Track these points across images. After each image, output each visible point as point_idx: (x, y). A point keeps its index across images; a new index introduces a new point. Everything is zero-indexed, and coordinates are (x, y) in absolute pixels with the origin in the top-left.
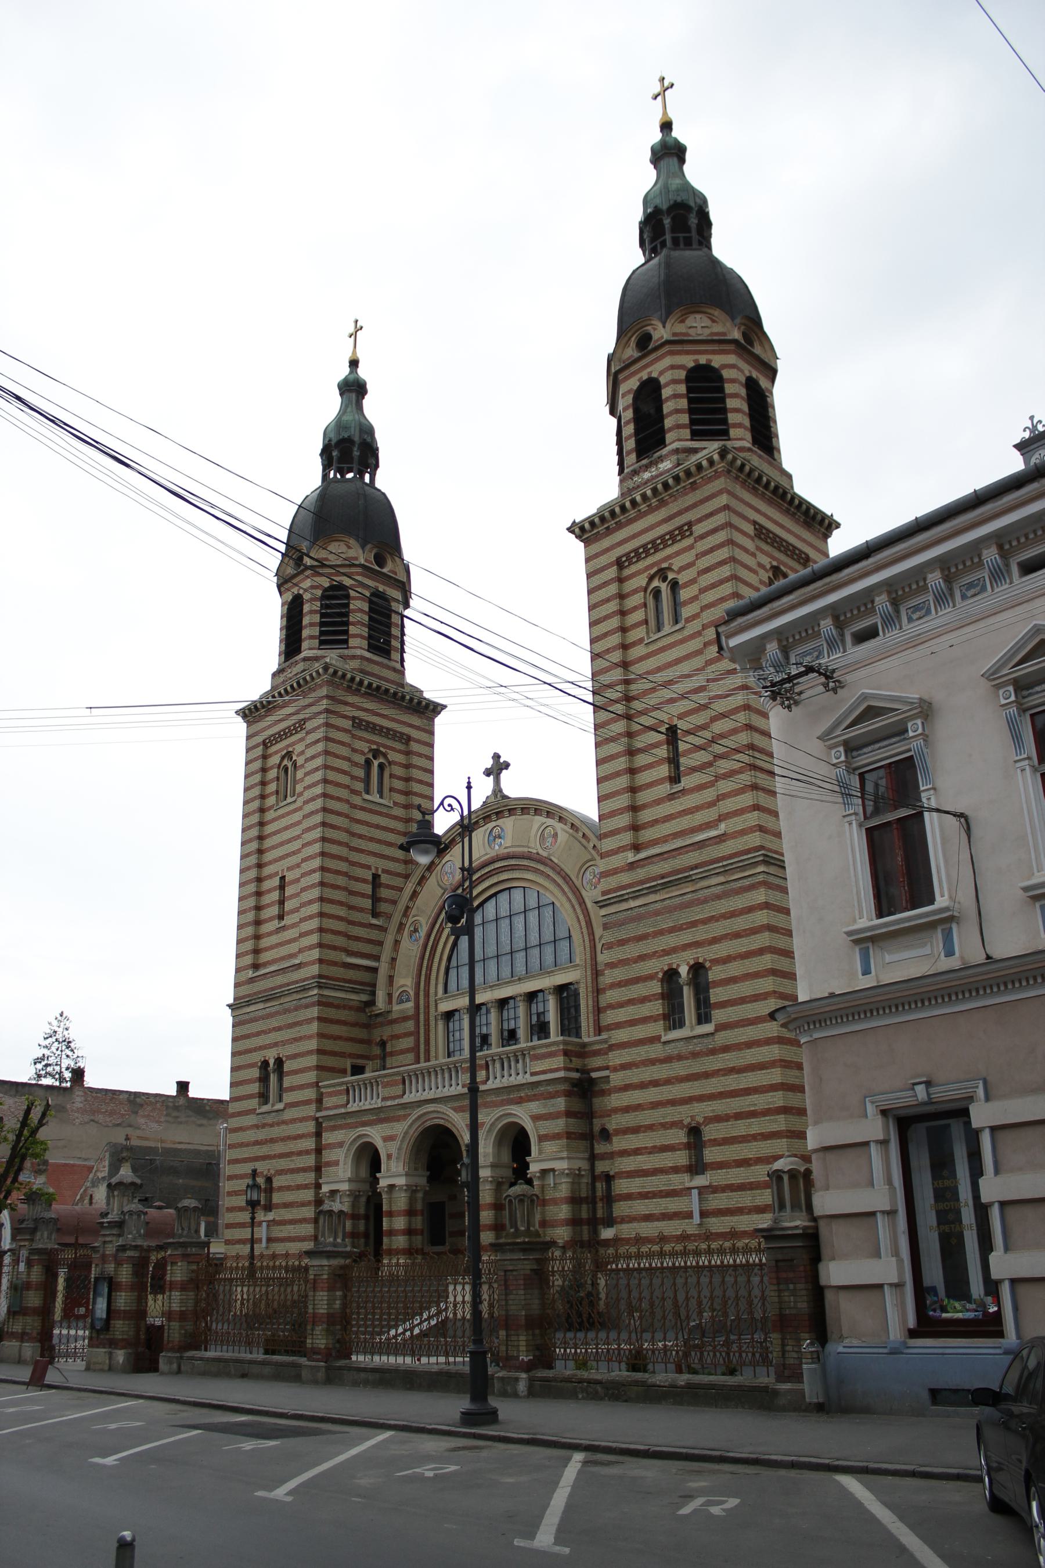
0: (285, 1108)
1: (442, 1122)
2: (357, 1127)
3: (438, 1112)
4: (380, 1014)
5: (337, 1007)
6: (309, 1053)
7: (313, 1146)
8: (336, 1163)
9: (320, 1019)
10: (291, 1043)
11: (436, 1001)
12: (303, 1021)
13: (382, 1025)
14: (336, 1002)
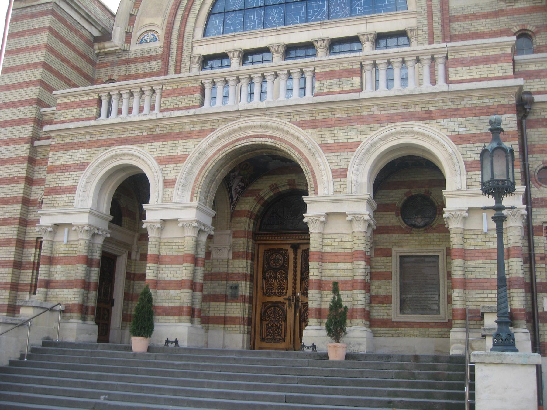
1: (268, 142)
2: (111, 145)
3: (266, 127)
4: (114, 53)
5: (70, 28)
6: (34, 65)
7: (23, 173)
8: (72, 190)
9: (50, 29)
11: (192, 43)
12: (25, 31)
13: (112, 64)
14: (70, 22)
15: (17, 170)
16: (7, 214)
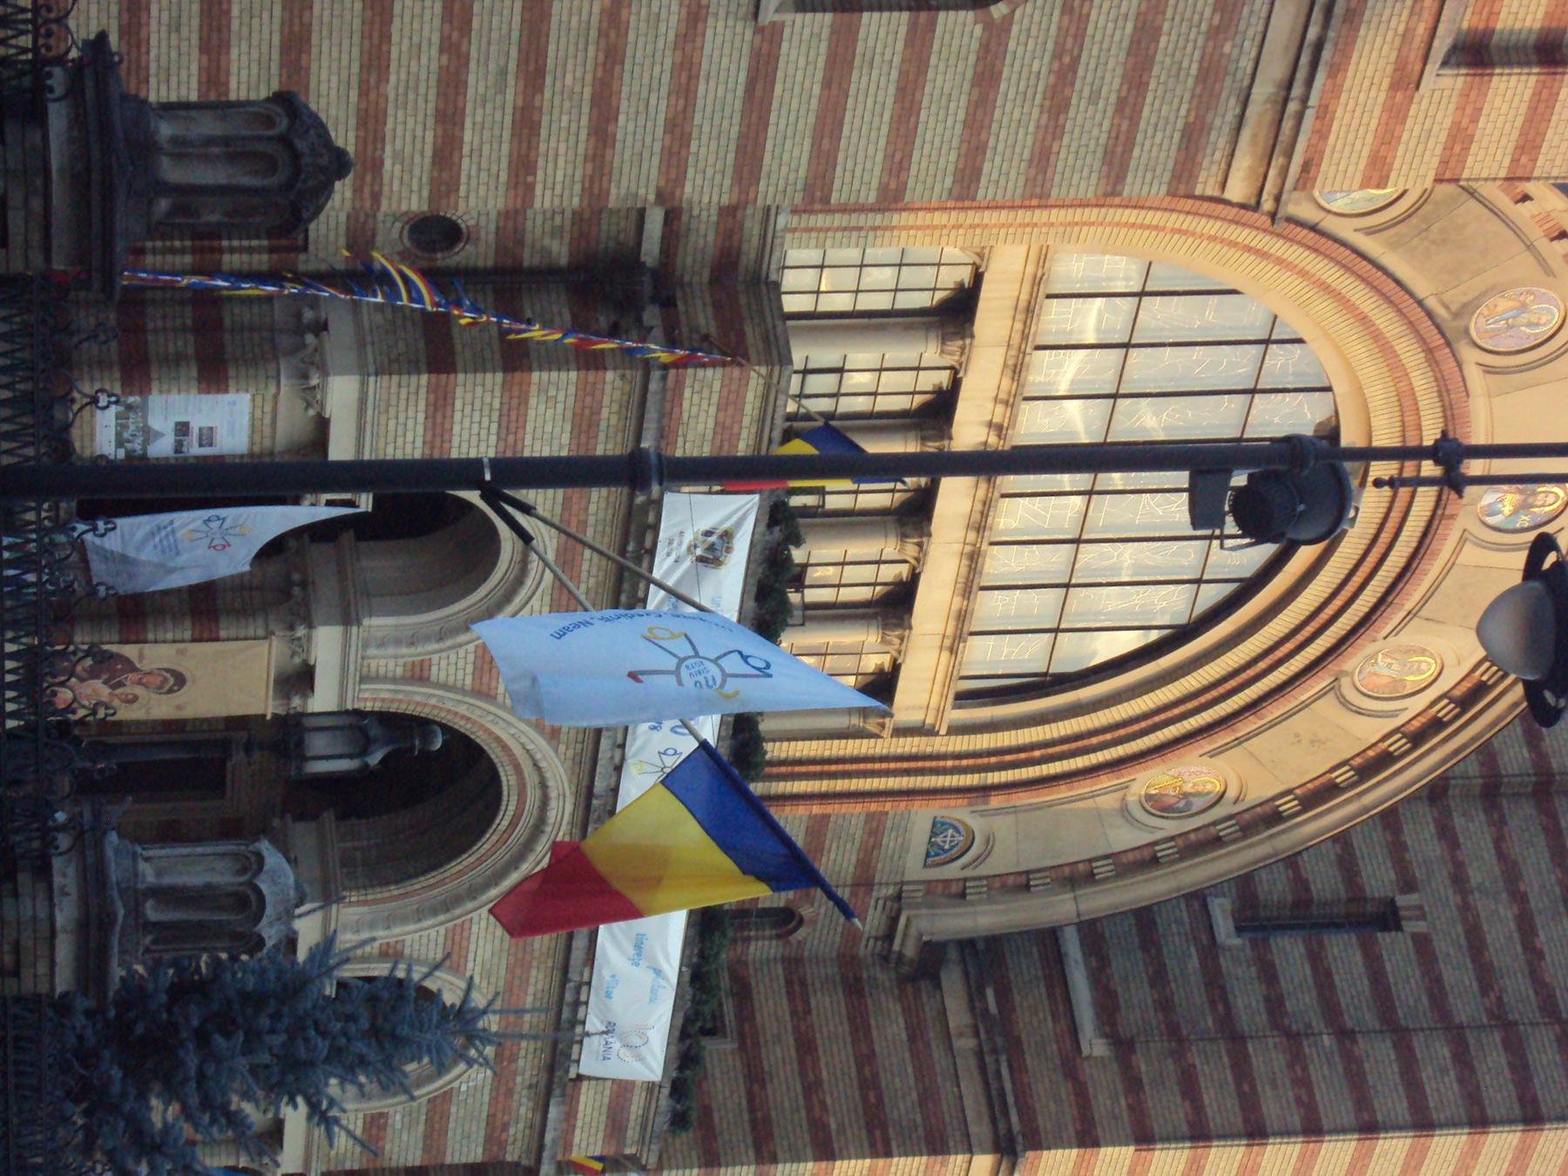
0: (759, 30)
10: (1058, 55)
15: (559, 178)
16: (398, 167)
